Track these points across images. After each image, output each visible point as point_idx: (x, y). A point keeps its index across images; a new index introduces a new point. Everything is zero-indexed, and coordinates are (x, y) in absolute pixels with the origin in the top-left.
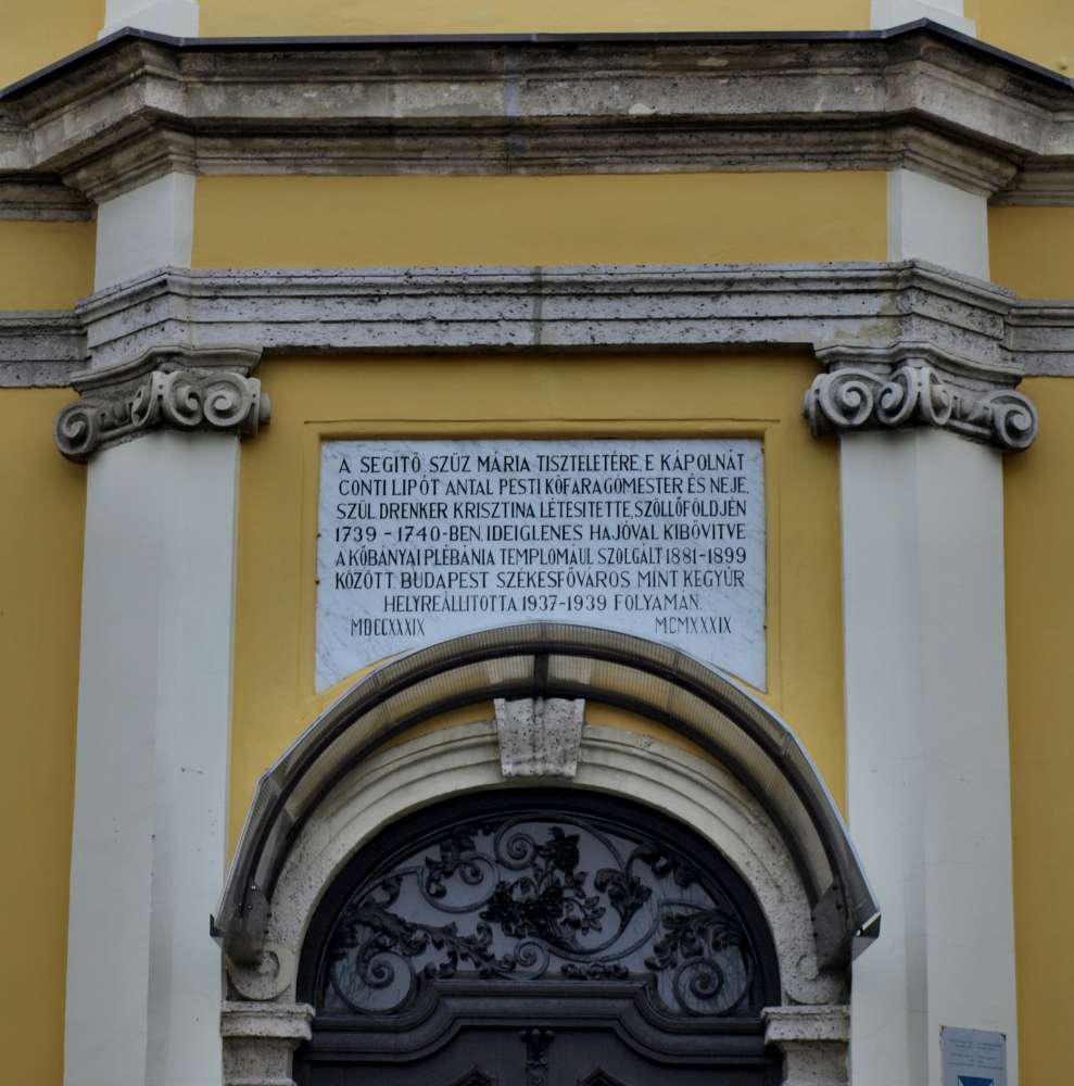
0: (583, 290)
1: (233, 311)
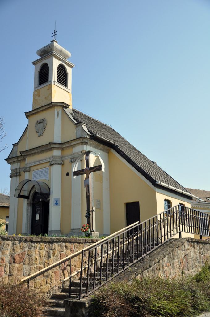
0: (41, 161)
1: (28, 165)
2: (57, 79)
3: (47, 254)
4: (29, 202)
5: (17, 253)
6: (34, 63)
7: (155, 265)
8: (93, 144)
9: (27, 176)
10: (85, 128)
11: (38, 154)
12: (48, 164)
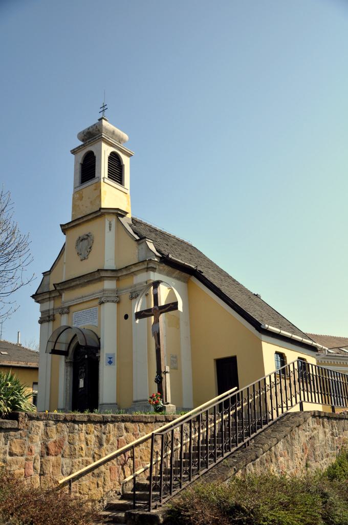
0: (85, 297)
2: (108, 174)
3: (97, 441)
4: (69, 361)
5: (52, 440)
6: (74, 152)
7: (265, 454)
8: (165, 270)
9: (64, 321)
10: (152, 246)
11: (82, 287)
12: (97, 302)
